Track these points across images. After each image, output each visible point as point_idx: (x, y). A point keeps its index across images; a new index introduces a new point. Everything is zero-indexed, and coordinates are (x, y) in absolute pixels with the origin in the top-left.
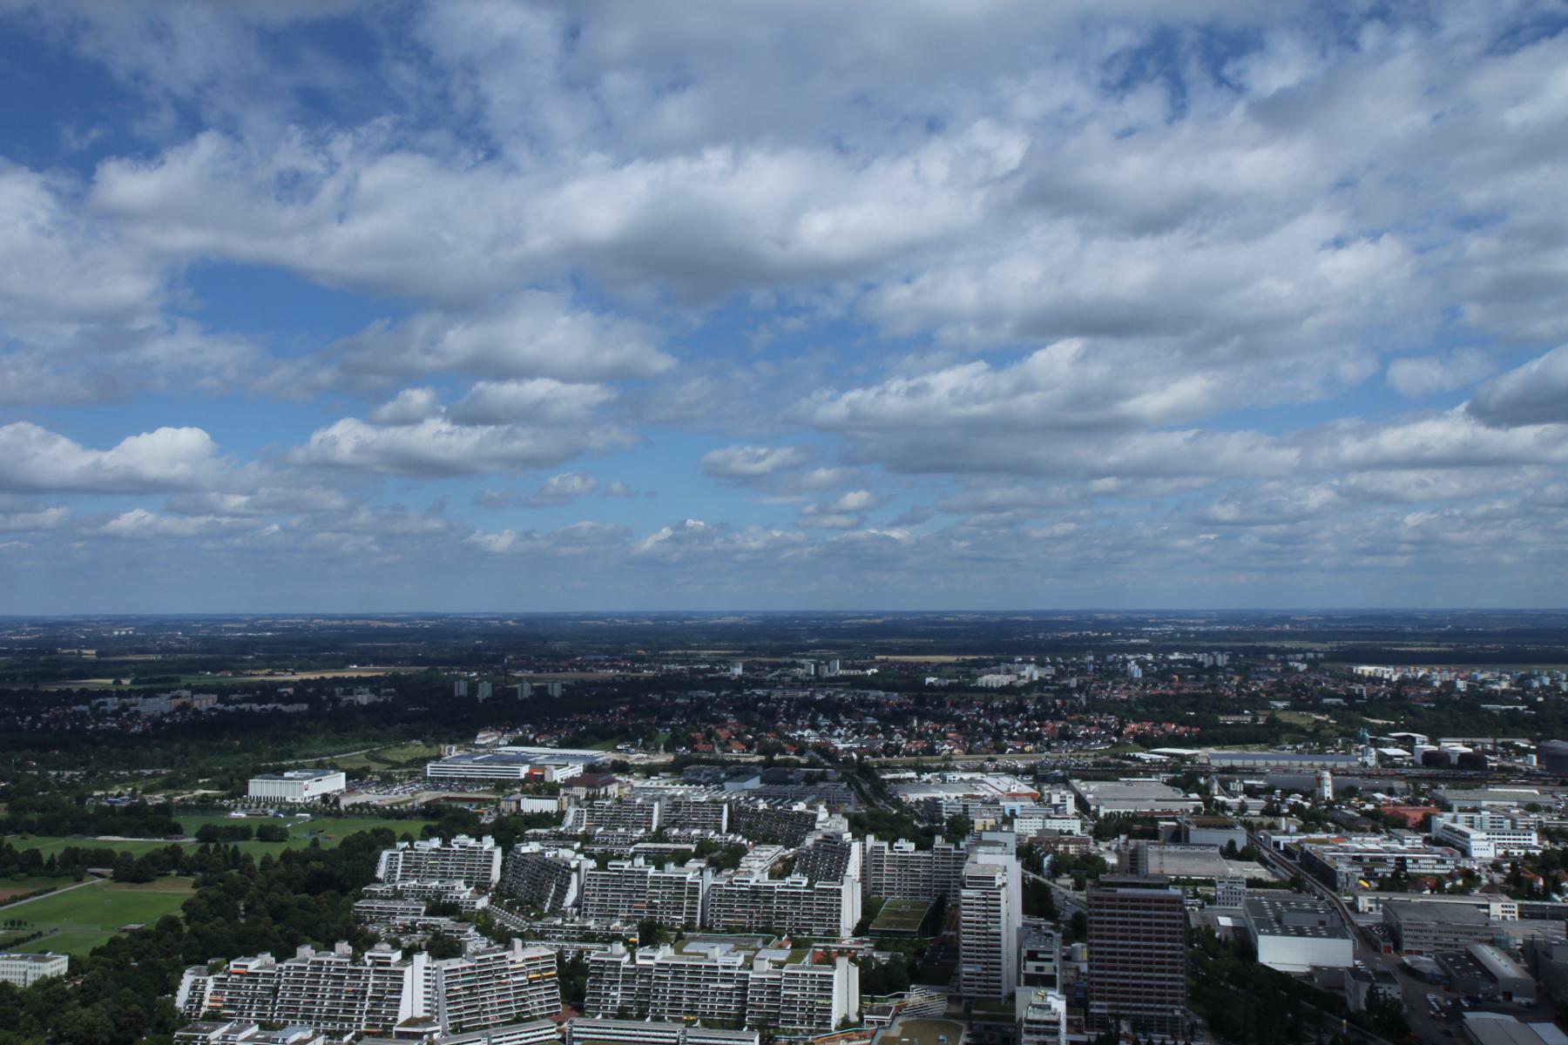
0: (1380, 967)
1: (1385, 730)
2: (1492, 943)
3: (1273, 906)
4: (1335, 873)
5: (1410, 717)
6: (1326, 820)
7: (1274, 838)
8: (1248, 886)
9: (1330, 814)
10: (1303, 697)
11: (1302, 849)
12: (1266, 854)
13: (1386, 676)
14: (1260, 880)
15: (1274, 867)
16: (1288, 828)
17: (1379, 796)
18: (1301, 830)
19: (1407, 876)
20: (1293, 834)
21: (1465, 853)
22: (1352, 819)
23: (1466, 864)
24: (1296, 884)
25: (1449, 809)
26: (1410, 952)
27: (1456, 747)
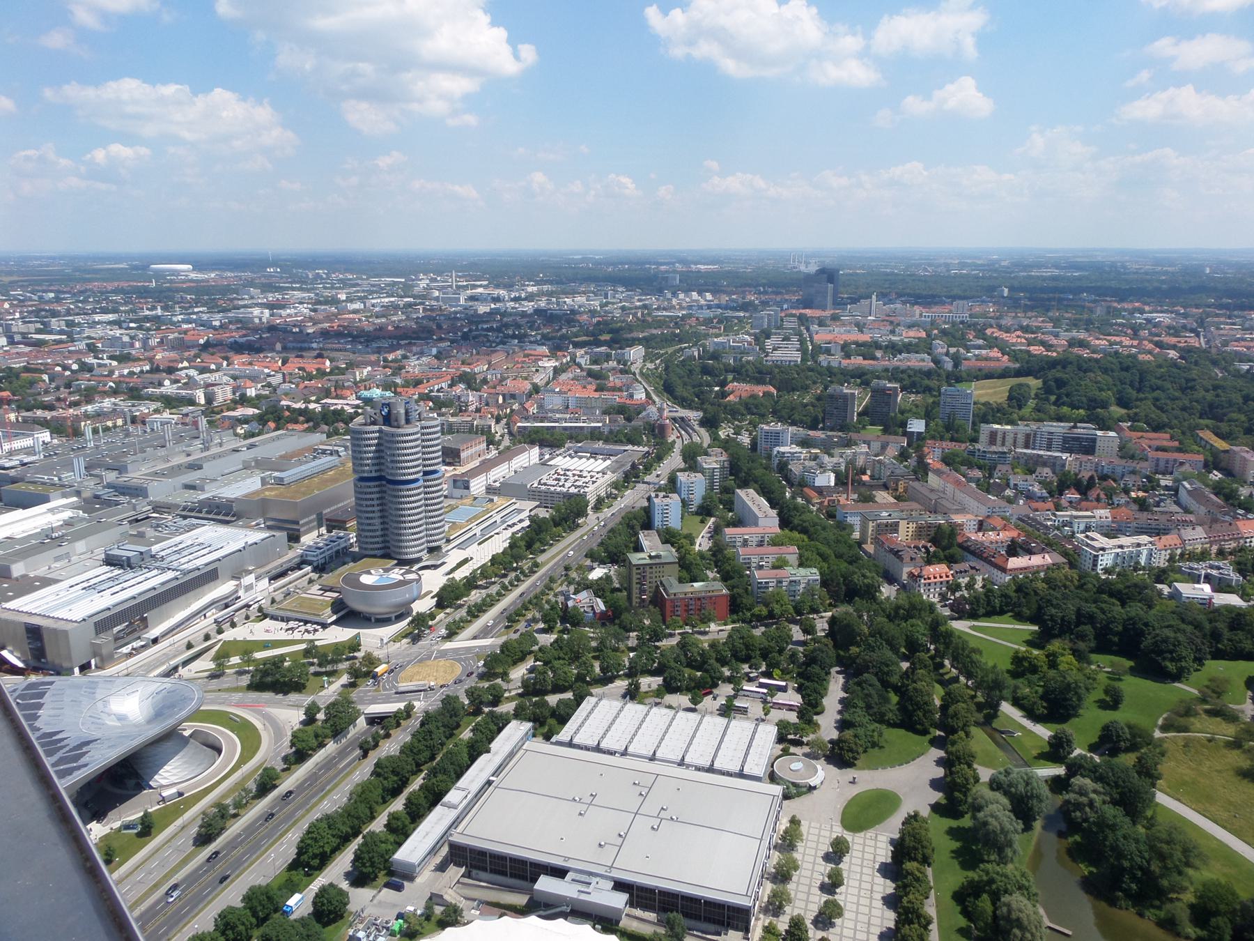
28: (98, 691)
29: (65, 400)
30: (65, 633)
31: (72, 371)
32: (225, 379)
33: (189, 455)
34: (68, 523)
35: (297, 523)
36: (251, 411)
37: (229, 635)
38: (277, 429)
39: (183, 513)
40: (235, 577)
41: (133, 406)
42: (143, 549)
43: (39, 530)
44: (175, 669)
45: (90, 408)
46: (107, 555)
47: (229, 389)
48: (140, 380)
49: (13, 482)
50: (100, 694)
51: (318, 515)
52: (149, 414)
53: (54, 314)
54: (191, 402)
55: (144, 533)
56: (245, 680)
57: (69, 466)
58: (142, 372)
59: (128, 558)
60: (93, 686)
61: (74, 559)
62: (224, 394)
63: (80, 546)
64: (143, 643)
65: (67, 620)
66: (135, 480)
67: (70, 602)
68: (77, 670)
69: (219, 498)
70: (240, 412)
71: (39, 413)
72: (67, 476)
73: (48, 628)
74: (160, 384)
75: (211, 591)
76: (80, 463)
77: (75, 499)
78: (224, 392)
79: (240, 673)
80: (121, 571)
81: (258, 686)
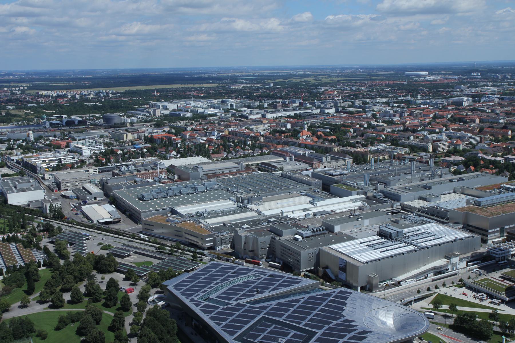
0: (54, 197)
1: (52, 115)
2: (90, 182)
3: (13, 182)
4: (36, 167)
5: (60, 109)
6: (32, 149)
7: (12, 158)
8: (2, 177)
9: (32, 147)
10: (20, 104)
11: (23, 160)
12: (9, 164)
13: (51, 95)
14: (7, 174)
15: (12, 168)
16: (17, 153)
17: (51, 138)
18: (22, 153)
19: (62, 165)
20: (19, 155)
21: (81, 154)
22: (41, 147)
23: (82, 158)
24: (22, 174)
25: (75, 140)
26: (64, 190)
27: (77, 118)
28: (373, 304)
29: (360, 143)
30: (357, 267)
31: (365, 128)
32: (444, 137)
33: (423, 180)
34: (360, 208)
35: (487, 231)
36: (460, 158)
37: (442, 291)
38: (476, 171)
39: (418, 213)
40: (446, 257)
41: (394, 149)
42: (399, 230)
43: (347, 210)
44: (410, 303)
45: (372, 148)
46: (380, 230)
47: (446, 144)
48: (398, 135)
49: (336, 183)
50: (374, 306)
51: (500, 229)
52: (401, 154)
53: (356, 98)
54: (425, 150)
55: (399, 221)
56: (451, 322)
57: (362, 177)
58: (398, 130)
59: (391, 234)
60: (371, 301)
61: (363, 228)
62: (444, 147)
63: (367, 222)
64: (393, 283)
65: (358, 261)
66: (394, 190)
67: (360, 251)
68: (359, 288)
69: (440, 207)
70: (452, 158)
71: (349, 148)
72: (361, 183)
73: (349, 263)
74: (409, 138)
75: (432, 262)
76: (368, 177)
77: (363, 196)
78: (444, 146)
79: (446, 317)
80: (386, 240)
81: (455, 328)
